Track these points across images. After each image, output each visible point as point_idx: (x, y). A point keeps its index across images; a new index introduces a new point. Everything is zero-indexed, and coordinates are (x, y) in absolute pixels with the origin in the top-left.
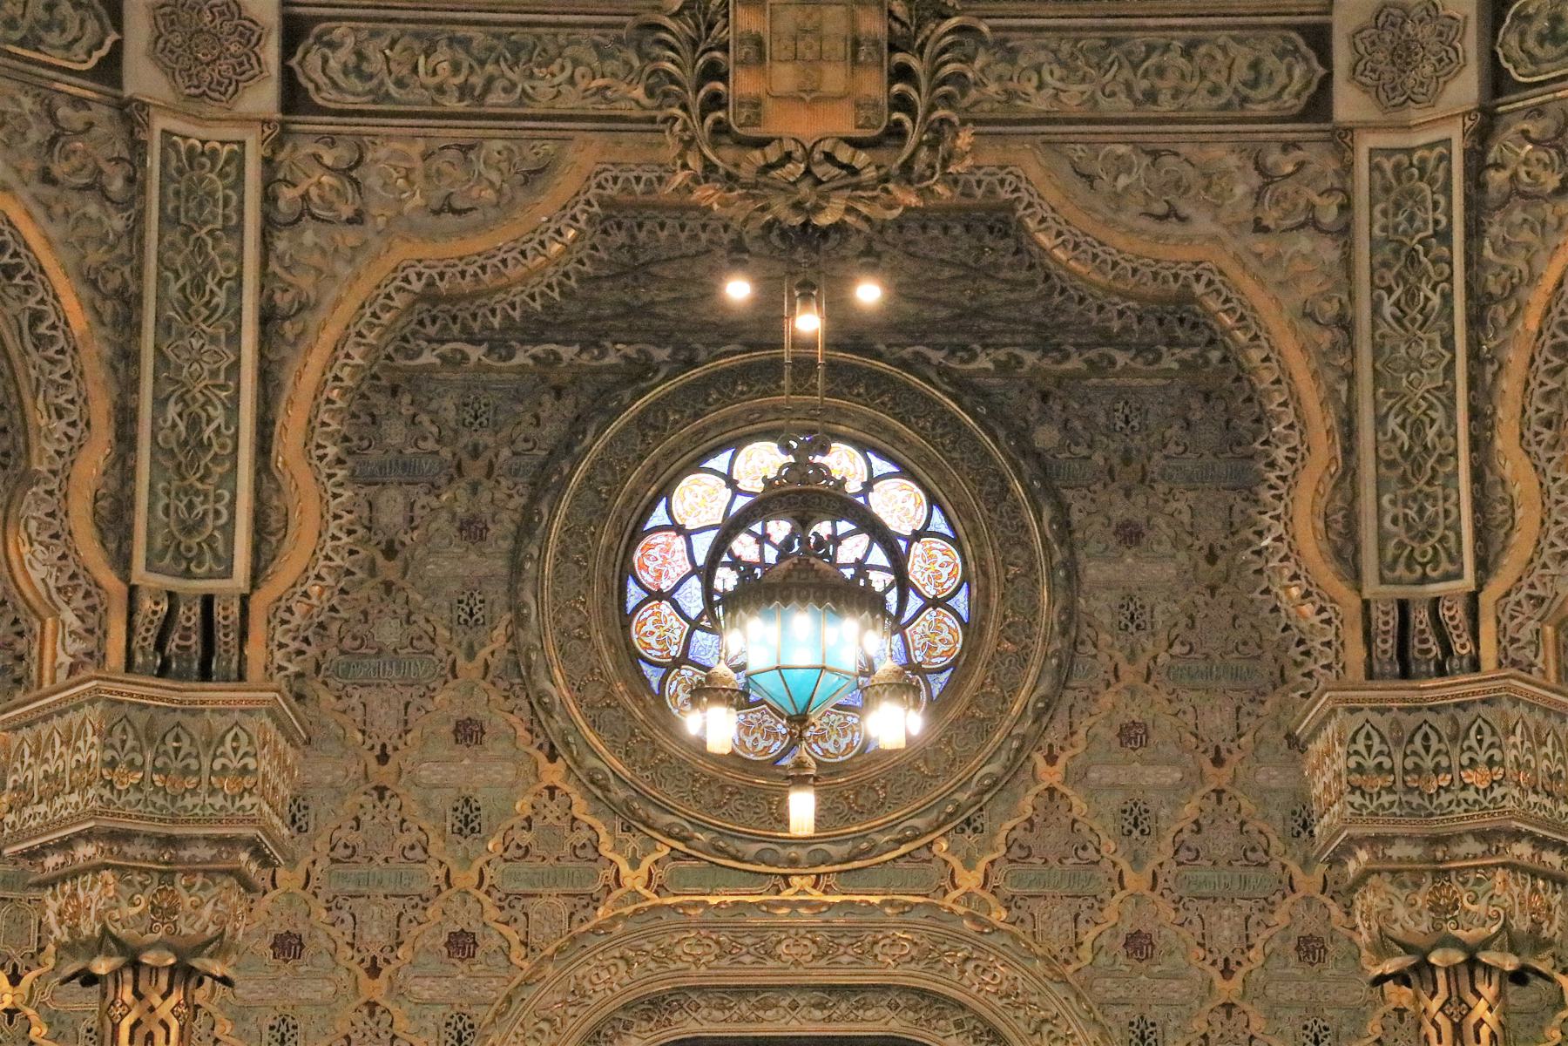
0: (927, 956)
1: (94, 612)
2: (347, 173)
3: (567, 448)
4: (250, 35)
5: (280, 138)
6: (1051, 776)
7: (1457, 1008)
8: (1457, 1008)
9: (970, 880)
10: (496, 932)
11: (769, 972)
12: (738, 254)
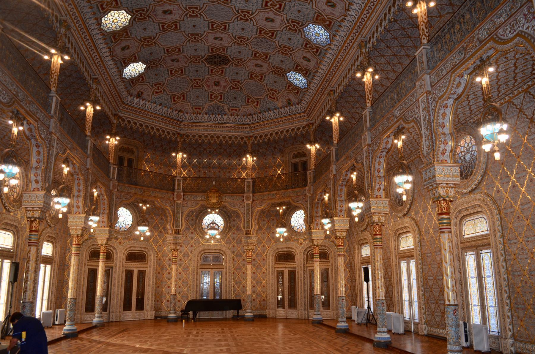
1: (172, 230)
3: (199, 215)
4: (181, 196)
7: (249, 253)
9: (223, 242)
12: (209, 208)
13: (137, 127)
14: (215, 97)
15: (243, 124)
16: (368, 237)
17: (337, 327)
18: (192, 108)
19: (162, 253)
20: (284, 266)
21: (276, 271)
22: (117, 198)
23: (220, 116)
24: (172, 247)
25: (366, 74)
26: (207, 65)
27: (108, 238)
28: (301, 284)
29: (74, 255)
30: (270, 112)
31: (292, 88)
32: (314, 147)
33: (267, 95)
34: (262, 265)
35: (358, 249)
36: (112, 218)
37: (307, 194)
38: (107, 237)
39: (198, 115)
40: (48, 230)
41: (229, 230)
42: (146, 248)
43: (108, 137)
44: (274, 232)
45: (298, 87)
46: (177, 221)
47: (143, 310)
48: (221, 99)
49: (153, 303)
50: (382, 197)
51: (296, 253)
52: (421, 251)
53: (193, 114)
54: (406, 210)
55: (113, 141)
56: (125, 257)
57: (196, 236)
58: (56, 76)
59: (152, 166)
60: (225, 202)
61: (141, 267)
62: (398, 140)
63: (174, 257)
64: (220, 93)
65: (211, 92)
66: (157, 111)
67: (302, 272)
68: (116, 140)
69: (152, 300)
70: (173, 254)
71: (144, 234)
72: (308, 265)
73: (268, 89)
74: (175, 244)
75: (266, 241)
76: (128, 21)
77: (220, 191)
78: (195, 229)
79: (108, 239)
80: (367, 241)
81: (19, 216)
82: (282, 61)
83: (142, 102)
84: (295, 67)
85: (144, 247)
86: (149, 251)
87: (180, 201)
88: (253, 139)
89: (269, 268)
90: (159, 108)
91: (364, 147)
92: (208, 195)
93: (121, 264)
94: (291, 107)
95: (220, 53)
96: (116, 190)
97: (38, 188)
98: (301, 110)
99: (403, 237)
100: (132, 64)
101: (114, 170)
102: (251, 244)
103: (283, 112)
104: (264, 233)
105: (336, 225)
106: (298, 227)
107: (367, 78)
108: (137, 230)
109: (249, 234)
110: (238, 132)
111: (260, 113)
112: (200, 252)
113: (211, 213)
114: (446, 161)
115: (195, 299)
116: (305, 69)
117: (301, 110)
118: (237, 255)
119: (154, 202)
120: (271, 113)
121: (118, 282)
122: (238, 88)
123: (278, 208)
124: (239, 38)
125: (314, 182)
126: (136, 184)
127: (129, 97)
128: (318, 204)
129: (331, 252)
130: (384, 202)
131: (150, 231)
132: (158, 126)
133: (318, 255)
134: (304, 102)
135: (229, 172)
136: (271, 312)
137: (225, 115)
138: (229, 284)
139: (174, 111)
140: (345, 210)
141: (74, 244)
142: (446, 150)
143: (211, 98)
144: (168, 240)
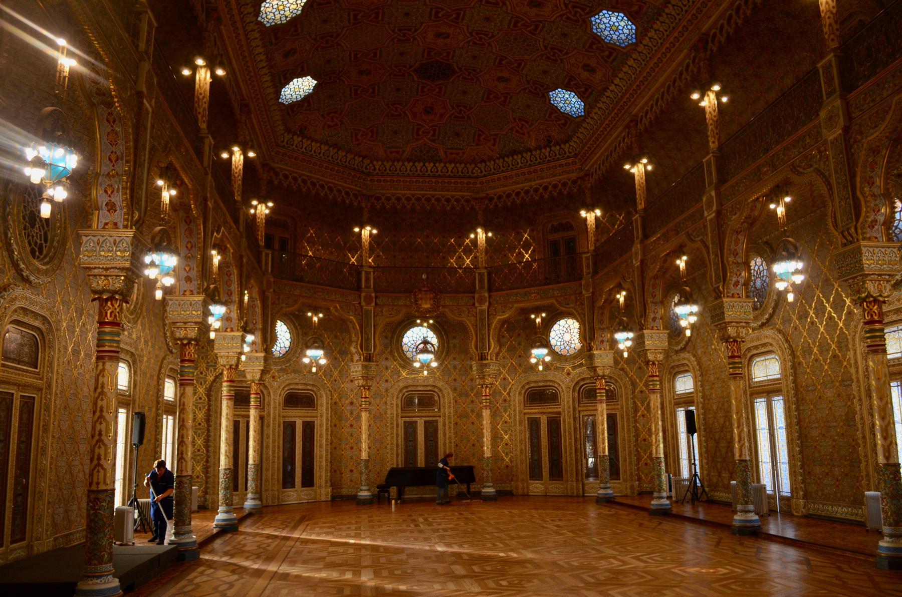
0: (434, 382)
1: (360, 355)
2: (382, 311)
4: (372, 298)
5: (375, 308)
6: (446, 363)
7: (486, 390)
8: (486, 390)
9: (438, 374)
10: (390, 379)
11: (418, 384)
12: (419, 318)
13: (290, 182)
14: (423, 132)
15: (470, 177)
16: (689, 361)
17: (652, 507)
18: (385, 151)
19: (340, 394)
20: (541, 411)
21: (526, 418)
22: (274, 302)
23: (432, 164)
24: (361, 382)
25: (708, 95)
26: (416, 79)
27: (262, 370)
28: (571, 439)
29: (227, 399)
30: (515, 157)
31: (555, 117)
32: (593, 215)
33: (512, 129)
34: (502, 410)
35: (669, 382)
36: (269, 338)
37: (584, 292)
38: (262, 368)
39: (396, 163)
40: (170, 358)
41: (447, 353)
42: (313, 385)
43: (255, 203)
44: (529, 356)
45: (568, 114)
46: (368, 340)
47: (313, 486)
48: (434, 135)
49: (329, 474)
50: (741, 296)
51: (560, 389)
52: (795, 381)
53: (388, 161)
54: (767, 316)
55: (262, 210)
56: (282, 402)
57: (393, 364)
58: (205, 103)
59: (318, 250)
60: (444, 307)
61: (307, 417)
62: (778, 204)
63: (363, 400)
64: (432, 126)
65: (418, 124)
66: (330, 158)
67: (572, 419)
68: (267, 207)
69: (326, 470)
70: (362, 395)
71: (317, 362)
72: (580, 409)
73: (514, 119)
74: (366, 378)
75: (509, 369)
76: (300, 9)
77: (437, 290)
78: (391, 353)
79: (263, 372)
80: (687, 368)
81: (134, 336)
82: (545, 72)
83: (306, 143)
84: (566, 82)
85: (311, 383)
86: (320, 389)
87: (371, 308)
88: (487, 202)
89: (515, 415)
90: (332, 151)
91: (708, 216)
92: (415, 296)
93: (277, 412)
94: (553, 148)
95: (442, 59)
96: (271, 290)
97: (191, 291)
98: (570, 153)
99: (758, 359)
100: (295, 80)
101: (268, 257)
102: (489, 375)
103: (538, 156)
104: (504, 358)
105: (647, 343)
106: (562, 347)
107: (710, 102)
108: (305, 356)
109: (486, 359)
110: (460, 191)
111: (498, 159)
112: (401, 391)
113: (421, 325)
114: (876, 238)
115: (395, 466)
116: (584, 84)
117: (570, 153)
118: (460, 395)
119: (329, 309)
120: (518, 158)
121: (274, 441)
122: (463, 117)
123: (533, 316)
124: (477, 34)
125: (595, 272)
126: (301, 280)
127: (286, 134)
128: (602, 308)
129: (621, 387)
130: (744, 304)
131: (326, 355)
132: (331, 183)
133: (604, 391)
134: (575, 139)
135: (444, 257)
136: (520, 485)
137: (441, 161)
138: (450, 442)
139: (356, 158)
140: (661, 318)
141: (225, 381)
142: (877, 221)
143: (418, 135)
144: (353, 372)
